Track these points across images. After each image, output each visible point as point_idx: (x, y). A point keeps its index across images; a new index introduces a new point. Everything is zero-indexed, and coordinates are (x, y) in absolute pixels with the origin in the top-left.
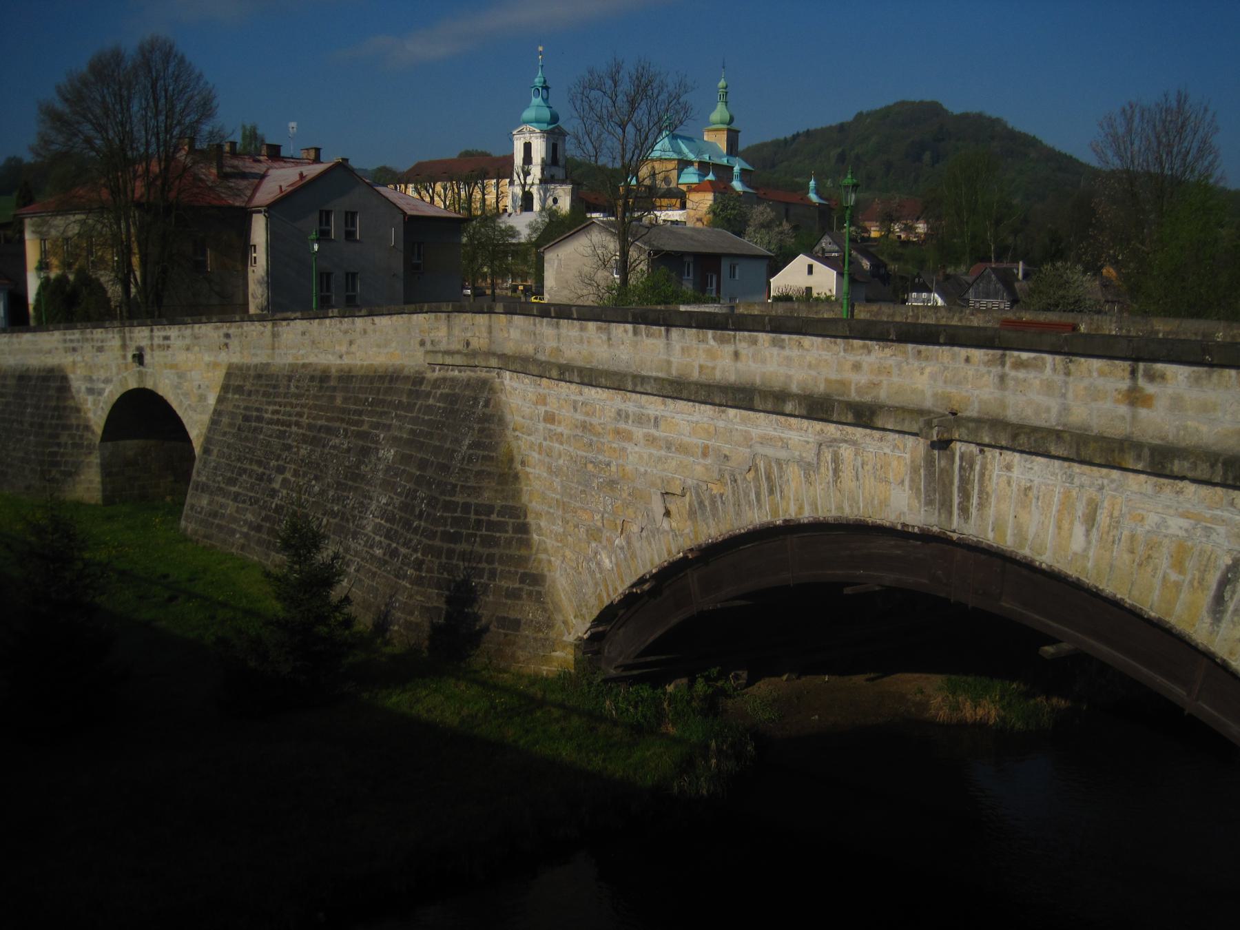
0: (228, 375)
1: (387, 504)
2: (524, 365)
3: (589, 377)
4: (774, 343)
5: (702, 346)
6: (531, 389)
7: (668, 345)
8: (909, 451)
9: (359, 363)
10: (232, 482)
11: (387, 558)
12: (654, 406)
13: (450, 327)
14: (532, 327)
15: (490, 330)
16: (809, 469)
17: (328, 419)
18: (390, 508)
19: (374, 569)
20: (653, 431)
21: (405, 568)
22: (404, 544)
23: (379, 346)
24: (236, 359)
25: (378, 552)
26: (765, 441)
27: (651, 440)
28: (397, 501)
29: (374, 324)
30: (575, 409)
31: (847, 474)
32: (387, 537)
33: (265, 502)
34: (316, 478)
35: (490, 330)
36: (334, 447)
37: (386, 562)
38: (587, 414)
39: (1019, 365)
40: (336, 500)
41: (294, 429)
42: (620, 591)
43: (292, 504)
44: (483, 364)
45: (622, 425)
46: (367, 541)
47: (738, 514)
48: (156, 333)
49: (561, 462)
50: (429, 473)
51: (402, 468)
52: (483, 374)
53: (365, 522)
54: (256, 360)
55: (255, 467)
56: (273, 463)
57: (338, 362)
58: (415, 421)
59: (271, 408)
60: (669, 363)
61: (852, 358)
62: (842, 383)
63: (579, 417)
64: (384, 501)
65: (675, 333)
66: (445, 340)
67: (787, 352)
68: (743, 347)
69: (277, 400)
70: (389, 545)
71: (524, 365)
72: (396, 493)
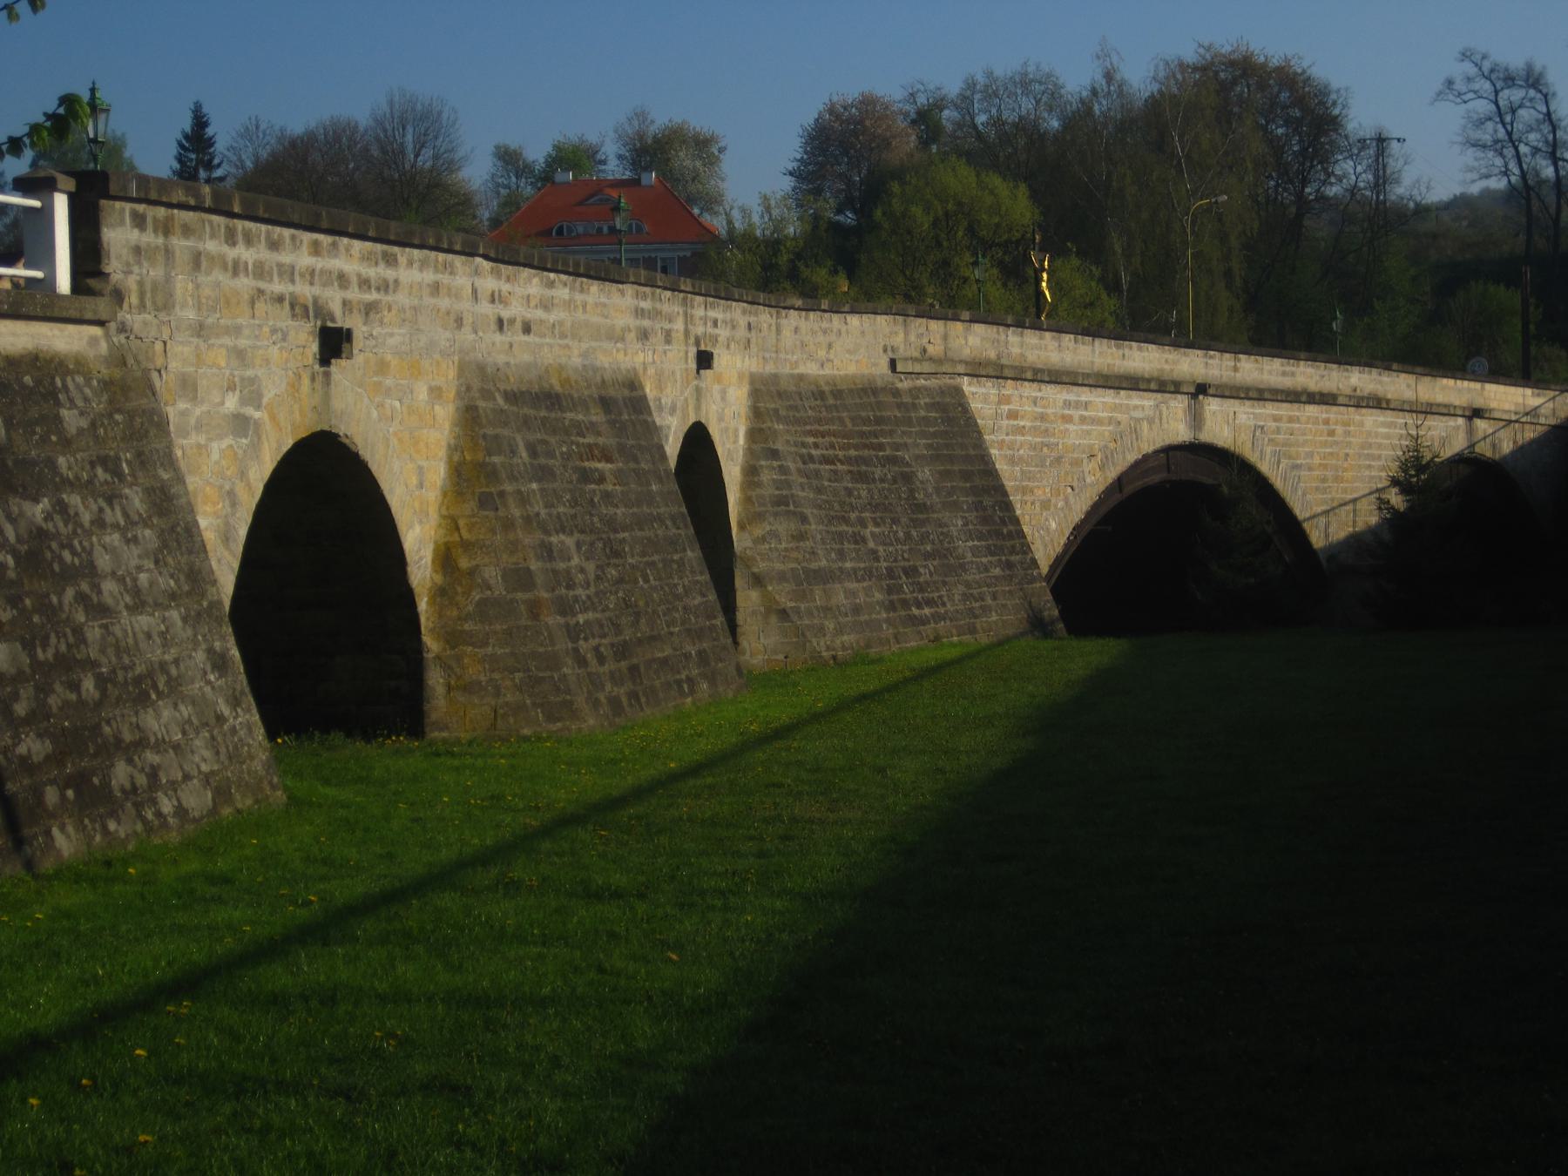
0: (755, 394)
1: (965, 525)
2: (996, 371)
4: (1140, 349)
5: (1110, 351)
6: (994, 391)
7: (1093, 351)
9: (836, 372)
10: (842, 555)
11: (1008, 572)
12: (1085, 395)
13: (906, 334)
14: (996, 336)
15: (945, 337)
16: (1151, 421)
17: (856, 447)
18: (971, 527)
19: (1007, 589)
20: (1084, 413)
21: (1030, 572)
22: (1011, 553)
23: (849, 352)
24: (754, 369)
25: (997, 571)
26: (1136, 407)
27: (1083, 420)
28: (972, 516)
29: (846, 323)
30: (1035, 404)
32: (992, 554)
33: (877, 569)
34: (895, 521)
35: (945, 337)
36: (882, 480)
38: (1044, 407)
39: (1211, 357)
40: (924, 538)
41: (840, 467)
42: (1062, 543)
43: (896, 560)
44: (950, 371)
45: (1067, 412)
46: (978, 568)
47: (1124, 458)
48: (699, 312)
49: (1021, 452)
51: (949, 485)
52: (947, 381)
53: (960, 551)
54: (770, 368)
55: (845, 528)
56: (853, 516)
57: (821, 372)
58: (923, 435)
59: (811, 440)
60: (1093, 363)
61: (1166, 356)
62: (1162, 370)
64: (960, 523)
65: (1097, 341)
66: (902, 347)
67: (1143, 354)
68: (1127, 351)
69: (808, 428)
70: (1000, 560)
71: (981, 370)
72: (964, 512)
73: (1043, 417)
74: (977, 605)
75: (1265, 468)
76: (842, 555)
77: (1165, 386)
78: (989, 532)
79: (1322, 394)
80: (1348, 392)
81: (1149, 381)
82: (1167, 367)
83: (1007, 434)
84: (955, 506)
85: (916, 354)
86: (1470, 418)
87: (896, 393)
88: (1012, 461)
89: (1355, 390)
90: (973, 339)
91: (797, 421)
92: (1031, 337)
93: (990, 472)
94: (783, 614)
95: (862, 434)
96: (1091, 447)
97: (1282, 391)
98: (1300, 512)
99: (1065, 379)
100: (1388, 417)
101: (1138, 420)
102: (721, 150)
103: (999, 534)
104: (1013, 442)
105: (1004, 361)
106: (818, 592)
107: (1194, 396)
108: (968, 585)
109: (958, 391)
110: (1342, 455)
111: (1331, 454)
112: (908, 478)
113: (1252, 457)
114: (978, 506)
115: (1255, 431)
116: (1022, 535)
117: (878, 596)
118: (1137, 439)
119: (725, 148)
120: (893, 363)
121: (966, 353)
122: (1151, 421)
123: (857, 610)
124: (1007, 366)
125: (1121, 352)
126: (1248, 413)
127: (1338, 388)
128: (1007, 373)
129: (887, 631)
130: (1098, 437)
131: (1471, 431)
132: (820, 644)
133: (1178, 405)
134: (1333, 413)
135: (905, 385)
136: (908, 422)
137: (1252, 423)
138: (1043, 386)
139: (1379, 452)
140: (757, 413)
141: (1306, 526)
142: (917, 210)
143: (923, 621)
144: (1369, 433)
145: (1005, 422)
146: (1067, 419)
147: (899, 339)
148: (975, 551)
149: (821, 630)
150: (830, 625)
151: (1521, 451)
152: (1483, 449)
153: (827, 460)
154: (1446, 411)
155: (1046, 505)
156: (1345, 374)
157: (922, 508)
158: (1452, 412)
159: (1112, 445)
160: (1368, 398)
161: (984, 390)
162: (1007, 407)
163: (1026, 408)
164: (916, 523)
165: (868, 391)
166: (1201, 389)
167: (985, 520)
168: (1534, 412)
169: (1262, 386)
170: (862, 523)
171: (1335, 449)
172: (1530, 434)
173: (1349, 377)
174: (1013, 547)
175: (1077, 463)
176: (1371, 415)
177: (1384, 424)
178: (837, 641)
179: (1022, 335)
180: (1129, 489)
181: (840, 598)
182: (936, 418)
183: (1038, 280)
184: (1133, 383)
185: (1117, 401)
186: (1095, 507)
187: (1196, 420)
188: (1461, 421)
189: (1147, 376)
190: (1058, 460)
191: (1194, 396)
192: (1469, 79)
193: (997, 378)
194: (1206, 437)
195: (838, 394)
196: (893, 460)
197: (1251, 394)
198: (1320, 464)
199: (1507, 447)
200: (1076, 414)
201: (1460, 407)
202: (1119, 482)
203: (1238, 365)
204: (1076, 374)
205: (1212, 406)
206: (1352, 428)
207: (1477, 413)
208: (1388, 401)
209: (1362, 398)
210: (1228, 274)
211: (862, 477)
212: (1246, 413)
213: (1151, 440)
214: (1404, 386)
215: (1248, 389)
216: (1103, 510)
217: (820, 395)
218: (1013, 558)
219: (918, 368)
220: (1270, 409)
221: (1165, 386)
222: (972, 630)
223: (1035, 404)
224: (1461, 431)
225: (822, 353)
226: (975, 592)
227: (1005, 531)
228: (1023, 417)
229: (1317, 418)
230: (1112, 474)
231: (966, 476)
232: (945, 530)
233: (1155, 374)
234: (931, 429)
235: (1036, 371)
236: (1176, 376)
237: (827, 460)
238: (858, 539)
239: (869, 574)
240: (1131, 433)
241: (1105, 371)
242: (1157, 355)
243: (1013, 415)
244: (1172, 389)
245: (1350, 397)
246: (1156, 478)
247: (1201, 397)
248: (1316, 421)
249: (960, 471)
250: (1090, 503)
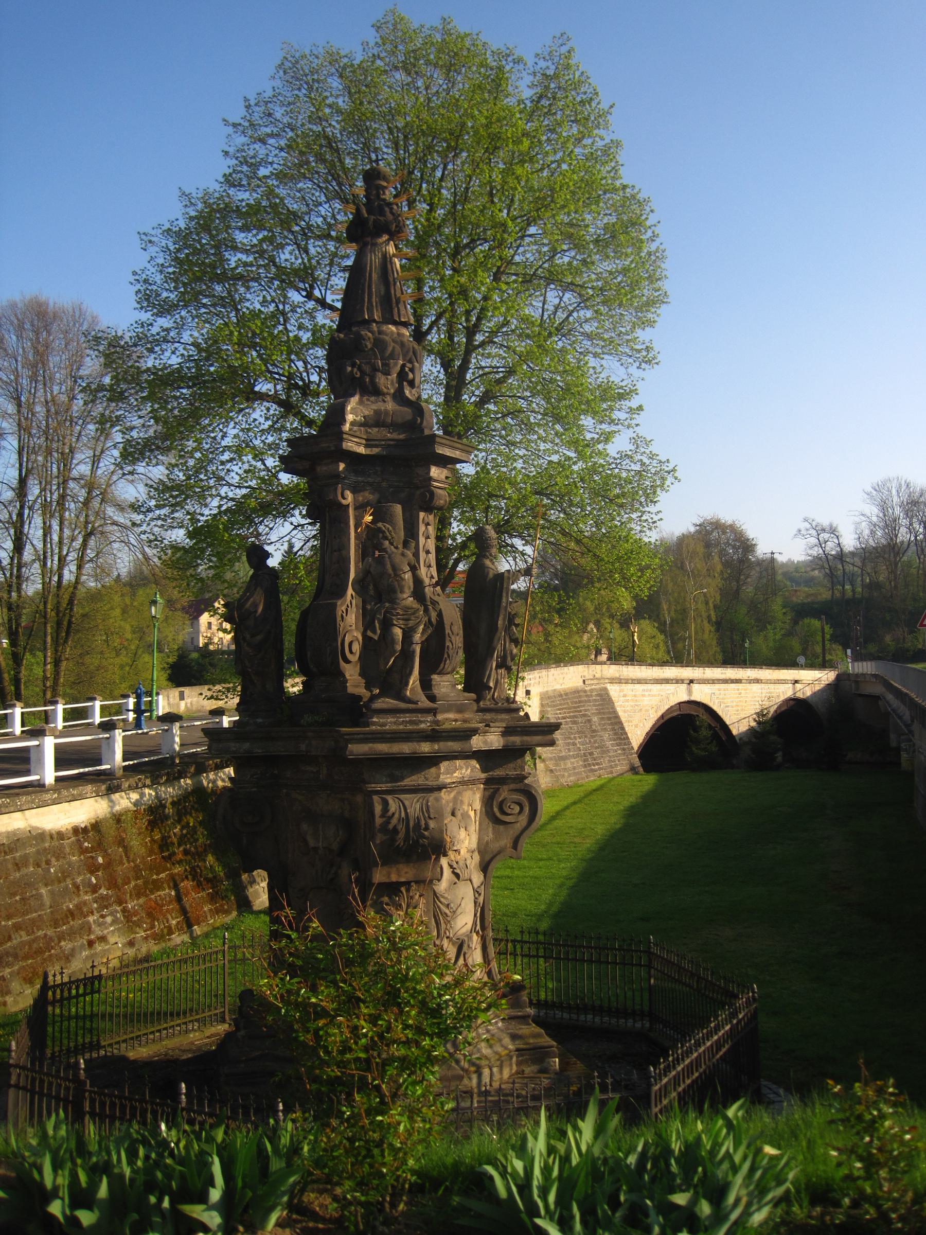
0: (542, 699)
2: (619, 681)
3: (639, 681)
10: (569, 750)
12: (649, 686)
34: (586, 737)
40: (595, 742)
50: (613, 721)
54: (546, 689)
58: (595, 705)
71: (613, 681)
73: (635, 696)
75: (715, 708)
76: (569, 750)
77: (679, 681)
84: (605, 729)
87: (585, 691)
88: (625, 712)
90: (613, 670)
91: (554, 706)
92: (631, 668)
93: (617, 717)
94: (551, 771)
95: (575, 707)
98: (728, 723)
103: (621, 739)
106: (562, 763)
107: (689, 684)
108: (610, 757)
109: (606, 689)
112: (589, 721)
113: (711, 705)
114: (613, 729)
116: (628, 738)
117: (581, 763)
120: (584, 681)
121: (609, 676)
122: (673, 694)
123: (574, 768)
129: (584, 775)
130: (655, 701)
131: (794, 689)
132: (563, 781)
133: (684, 687)
135: (588, 688)
136: (589, 701)
140: (542, 705)
141: (731, 727)
142: (588, 603)
143: (596, 771)
146: (644, 696)
147: (586, 674)
148: (613, 745)
149: (563, 776)
150: (566, 774)
151: (814, 694)
152: (800, 695)
153: (564, 718)
154: (784, 682)
155: (636, 726)
157: (594, 731)
164: (592, 737)
165: (577, 691)
166: (691, 681)
167: (615, 734)
168: (819, 679)
170: (575, 738)
172: (818, 688)
175: (647, 711)
178: (568, 779)
180: (666, 718)
181: (569, 765)
183: (633, 636)
184: (667, 681)
186: (654, 725)
187: (690, 692)
188: (790, 685)
190: (641, 710)
191: (689, 684)
192: (807, 530)
194: (693, 698)
195: (566, 694)
196: (585, 715)
199: (809, 693)
200: (647, 693)
202: (662, 716)
205: (695, 687)
207: (796, 682)
210: (709, 617)
211: (574, 723)
213: (674, 701)
216: (657, 726)
217: (561, 695)
220: (717, 686)
221: (679, 681)
222: (612, 773)
225: (561, 681)
230: (660, 714)
231: (609, 719)
235: (633, 680)
236: (682, 677)
237: (564, 718)
238: (574, 744)
239: (578, 756)
243: (625, 696)
246: (675, 714)
248: (734, 689)
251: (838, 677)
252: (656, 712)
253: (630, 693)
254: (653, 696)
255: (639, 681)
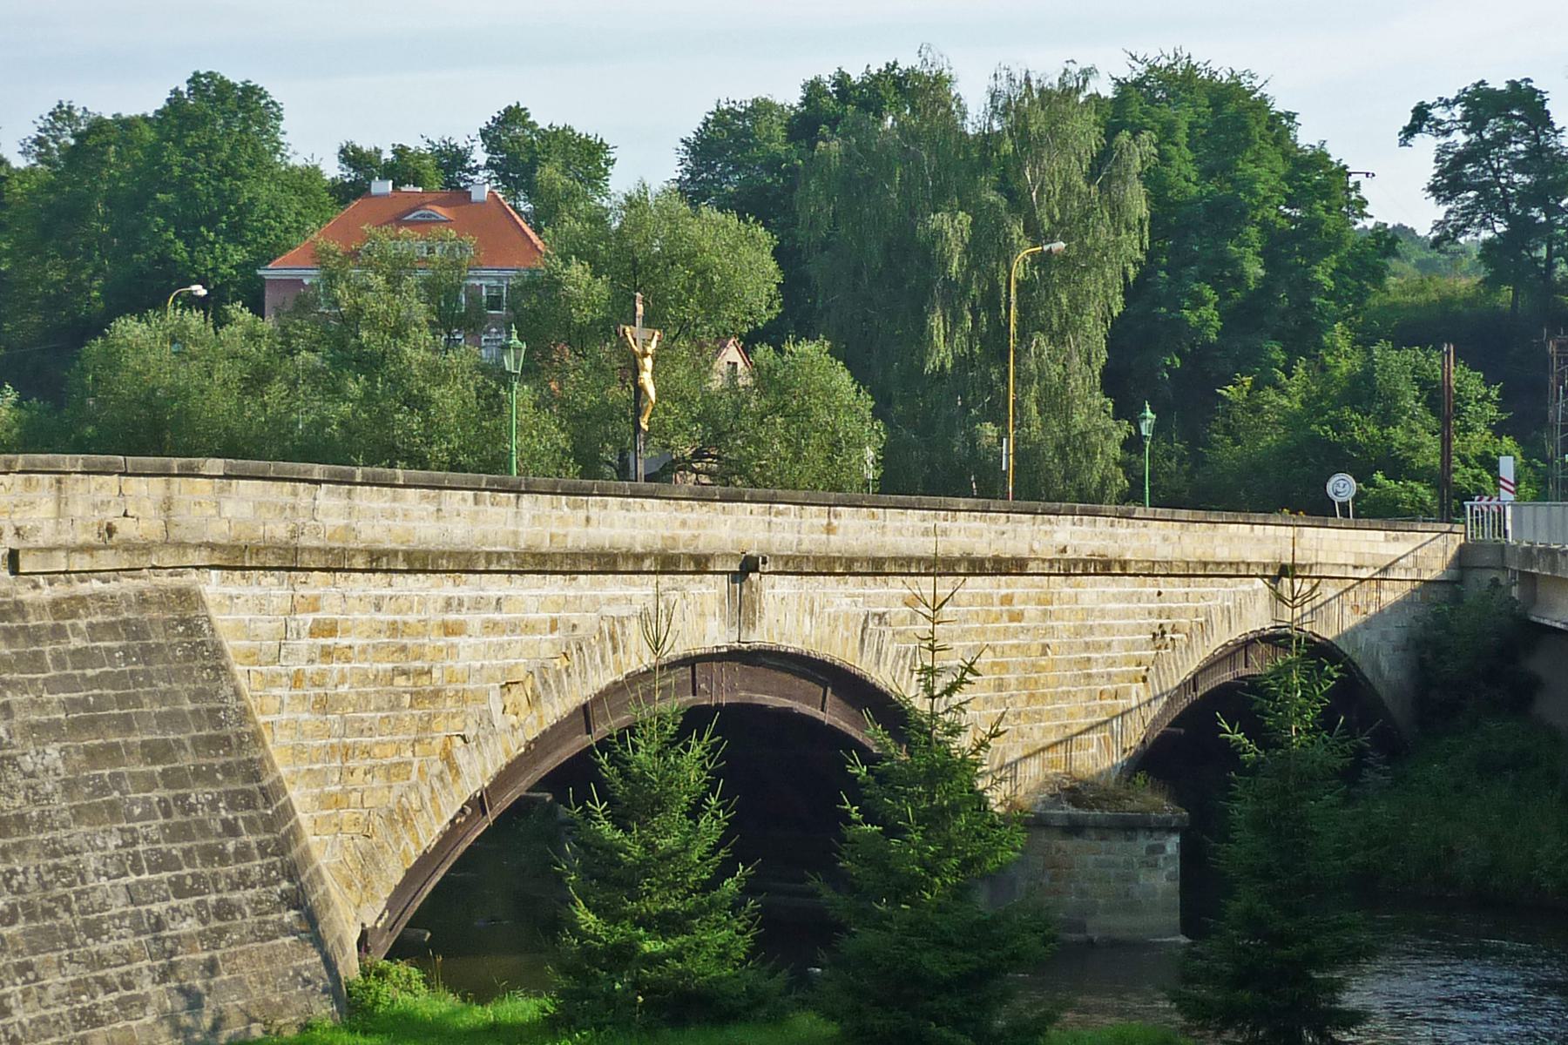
3: (420, 563)
4: (622, 507)
5: (556, 513)
6: (285, 591)
8: (711, 590)
12: (495, 586)
13: (60, 502)
14: (291, 500)
15: (167, 505)
20: (497, 616)
22: (235, 887)
26: (613, 600)
27: (491, 627)
31: (676, 616)
35: (167, 505)
37: (221, 933)
39: (778, 513)
44: (170, 563)
45: (451, 617)
46: (133, 926)
51: (107, 772)
52: (165, 580)
60: (515, 533)
61: (681, 516)
63: (385, 617)
64: (114, 842)
65: (526, 499)
67: (632, 514)
68: (594, 512)
73: (394, 628)
74: (114, 996)
78: (187, 853)
79: (997, 560)
80: (1052, 554)
81: (640, 558)
82: (685, 533)
83: (311, 661)
85: (92, 538)
86: (1276, 579)
89: (1064, 550)
96: (510, 670)
97: (919, 560)
99: (444, 564)
100: (1127, 585)
101: (621, 621)
102: (610, 163)
103: (213, 855)
104: (322, 674)
105: (305, 541)
109: (186, 597)
110: (1036, 646)
111: (1018, 646)
113: (864, 665)
115: (866, 621)
118: (615, 649)
119: (614, 160)
121: (218, 532)
124: (311, 550)
125: (582, 514)
126: (853, 596)
127: (1032, 550)
128: (306, 560)
133: (711, 590)
134: (1018, 586)
136: (35, 662)
137: (862, 610)
138: (398, 579)
139: (1107, 639)
144: (1089, 612)
145: (306, 641)
146: (449, 630)
154: (1235, 571)
156: (1047, 527)
158: (1243, 572)
159: (560, 664)
160: (1085, 562)
161: (257, 591)
162: (310, 617)
163: (356, 615)
166: (749, 565)
169: (881, 554)
171: (1023, 639)
173: (1052, 532)
174: (244, 874)
176: (1094, 585)
177: (1116, 598)
179: (349, 494)
182: (110, 651)
183: (636, 371)
184: (606, 562)
185: (571, 593)
187: (744, 610)
189: (639, 549)
193: (289, 569)
194: (759, 637)
197: (856, 568)
198: (994, 664)
200: (474, 619)
201: (1258, 564)
203: (835, 522)
204: (470, 556)
205: (775, 591)
206: (1056, 607)
207: (1286, 571)
208: (1124, 564)
209: (1075, 562)
212: (842, 596)
214: (1156, 540)
215: (851, 561)
218: (236, 896)
219: (81, 562)
223: (378, 608)
224: (1260, 595)
226: (112, 973)
227: (231, 846)
228: (346, 632)
229: (991, 595)
230: (556, 709)
232: (65, 861)
233: (659, 545)
234: (90, 672)
236: (702, 547)
240: (602, 639)
241: (545, 547)
242: (663, 515)
244: (692, 568)
245: (1051, 562)
247: (754, 577)
248: (987, 599)
249: (144, 744)
250: (503, 761)
251: (1463, 561)
252: (533, 702)
253: (362, 616)
254: (513, 628)
255: (420, 563)
